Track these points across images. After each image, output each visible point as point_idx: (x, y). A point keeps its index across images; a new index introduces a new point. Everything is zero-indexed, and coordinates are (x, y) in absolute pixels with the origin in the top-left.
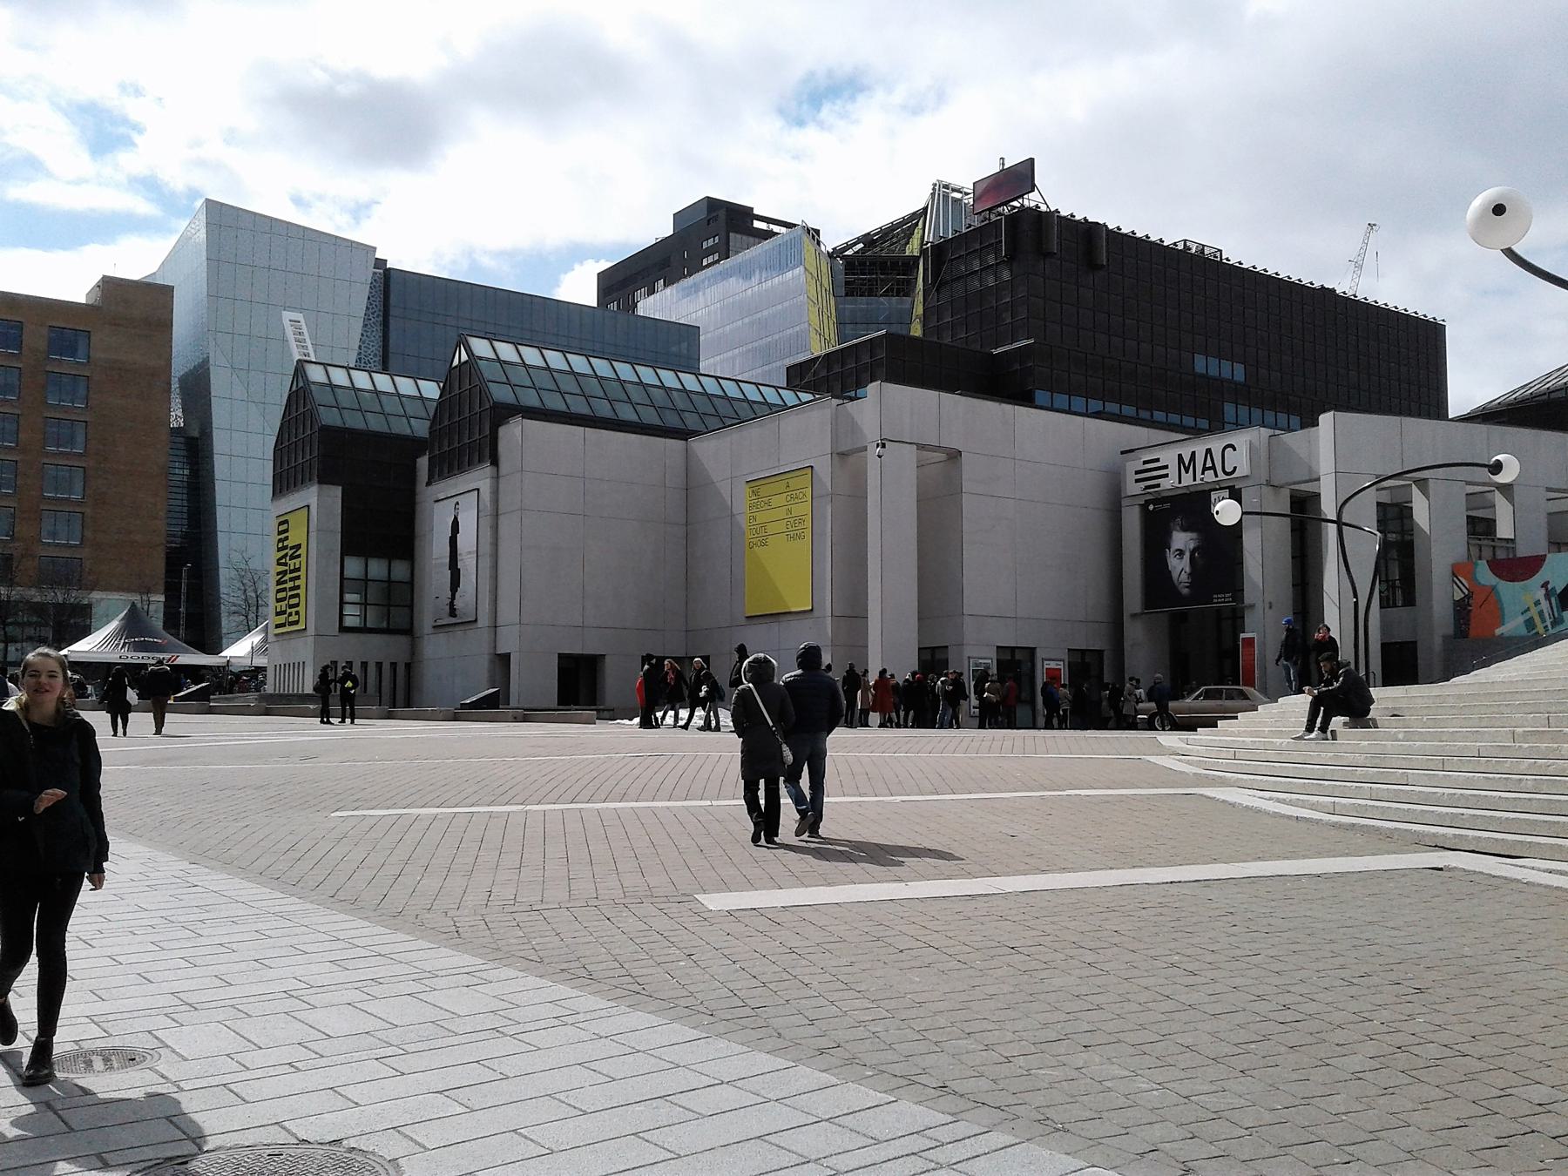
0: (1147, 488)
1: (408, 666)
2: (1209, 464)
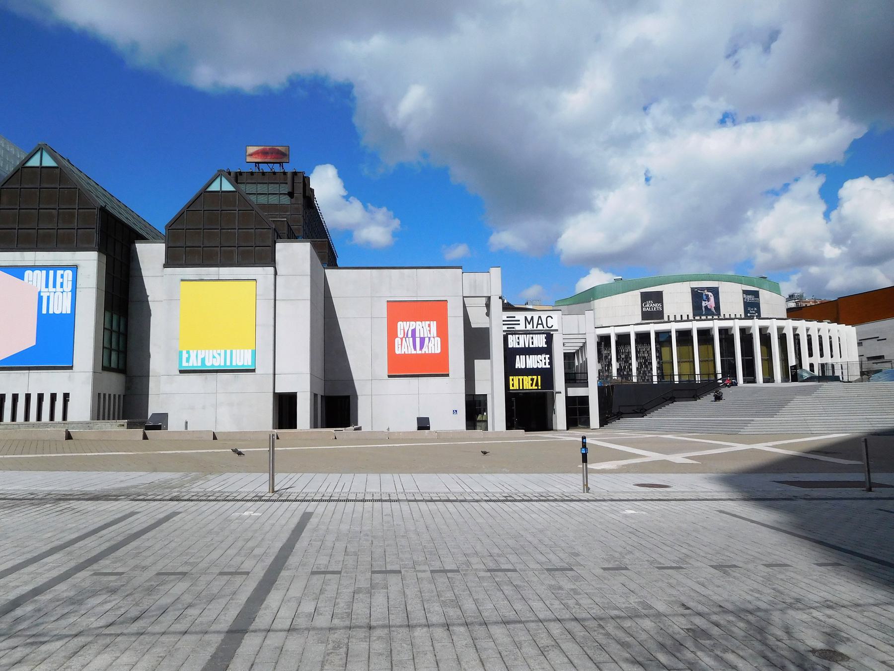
0: (508, 328)
2: (540, 322)
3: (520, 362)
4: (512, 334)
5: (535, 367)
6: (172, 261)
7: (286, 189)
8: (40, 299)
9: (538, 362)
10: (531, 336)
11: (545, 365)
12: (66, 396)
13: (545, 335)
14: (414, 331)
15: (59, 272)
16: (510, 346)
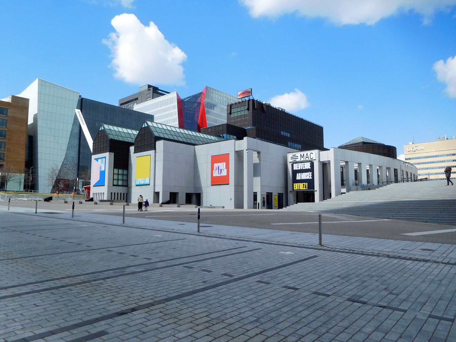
1: (127, 194)
2: (307, 156)
3: (299, 176)
4: (295, 163)
5: (305, 179)
6: (136, 152)
7: (246, 107)
8: (100, 166)
9: (306, 176)
10: (304, 163)
11: (310, 177)
12: (104, 193)
13: (310, 163)
14: (219, 167)
15: (103, 159)
16: (294, 169)
